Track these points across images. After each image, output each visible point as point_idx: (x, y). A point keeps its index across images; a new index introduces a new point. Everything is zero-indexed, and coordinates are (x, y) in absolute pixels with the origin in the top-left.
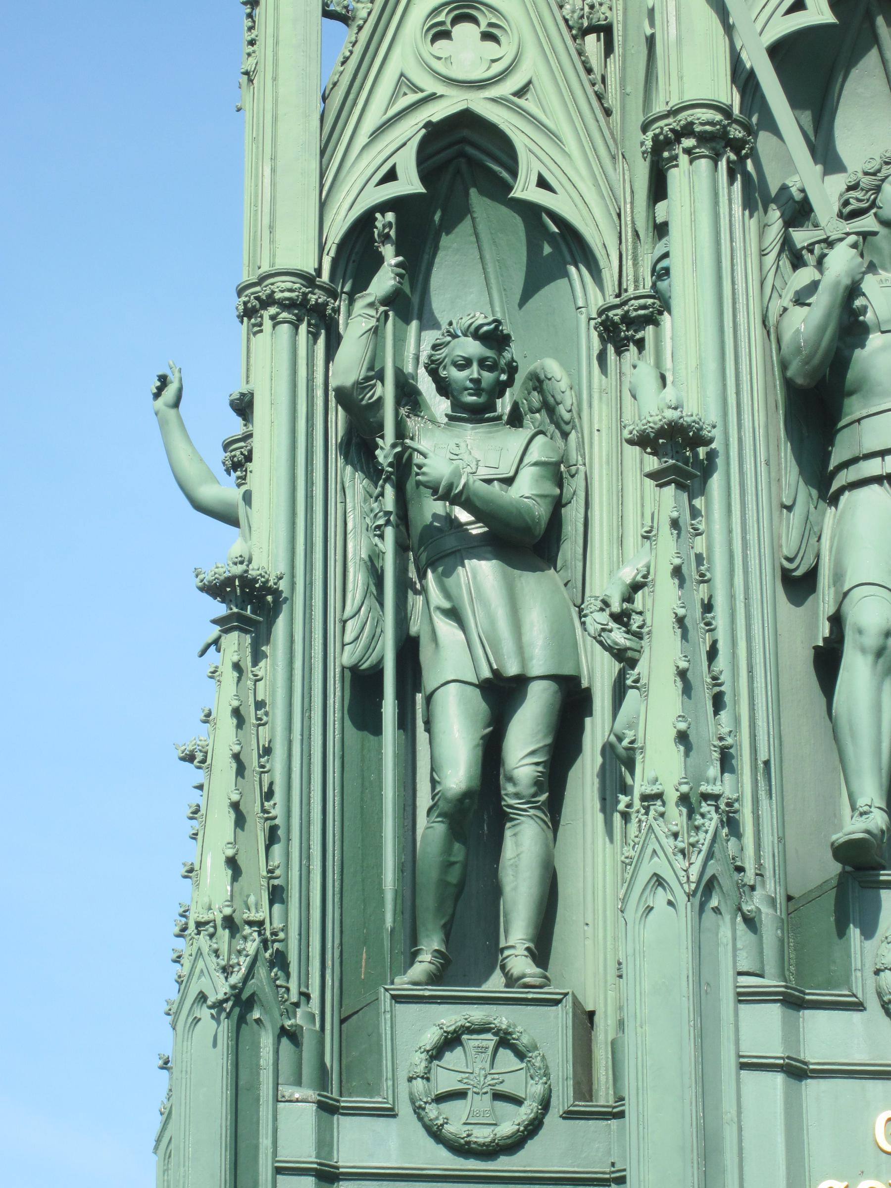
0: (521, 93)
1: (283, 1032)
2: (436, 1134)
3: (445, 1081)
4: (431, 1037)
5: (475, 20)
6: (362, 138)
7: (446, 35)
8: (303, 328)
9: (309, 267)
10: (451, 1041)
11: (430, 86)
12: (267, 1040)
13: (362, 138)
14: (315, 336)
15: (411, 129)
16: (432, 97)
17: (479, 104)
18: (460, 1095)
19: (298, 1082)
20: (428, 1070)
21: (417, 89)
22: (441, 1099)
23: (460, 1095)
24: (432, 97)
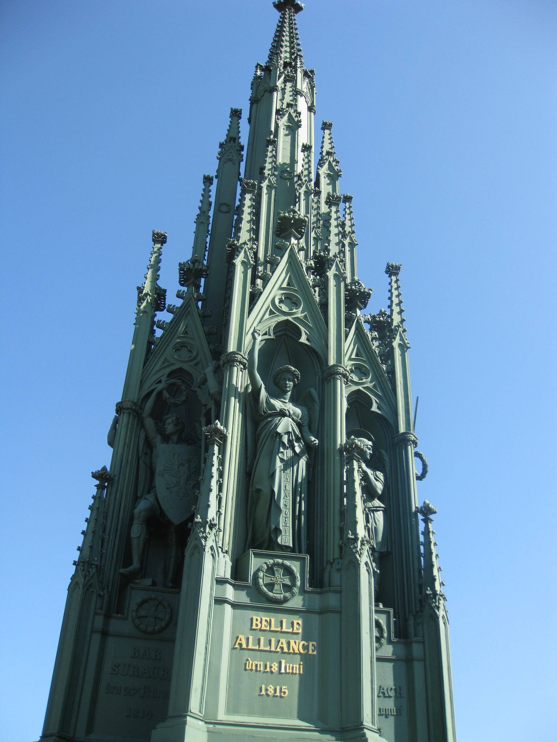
0: (197, 364)
1: (99, 595)
2: (137, 627)
3: (142, 613)
4: (139, 601)
5: (186, 347)
6: (154, 372)
7: (179, 350)
8: (131, 416)
9: (135, 400)
10: (144, 602)
11: (173, 361)
12: (95, 596)
13: (154, 372)
14: (135, 418)
15: (168, 371)
16: (173, 364)
17: (185, 366)
18: (146, 617)
19: (102, 609)
20: (138, 609)
21: (169, 362)
22: (140, 618)
23: (146, 617)
24: (173, 364)
